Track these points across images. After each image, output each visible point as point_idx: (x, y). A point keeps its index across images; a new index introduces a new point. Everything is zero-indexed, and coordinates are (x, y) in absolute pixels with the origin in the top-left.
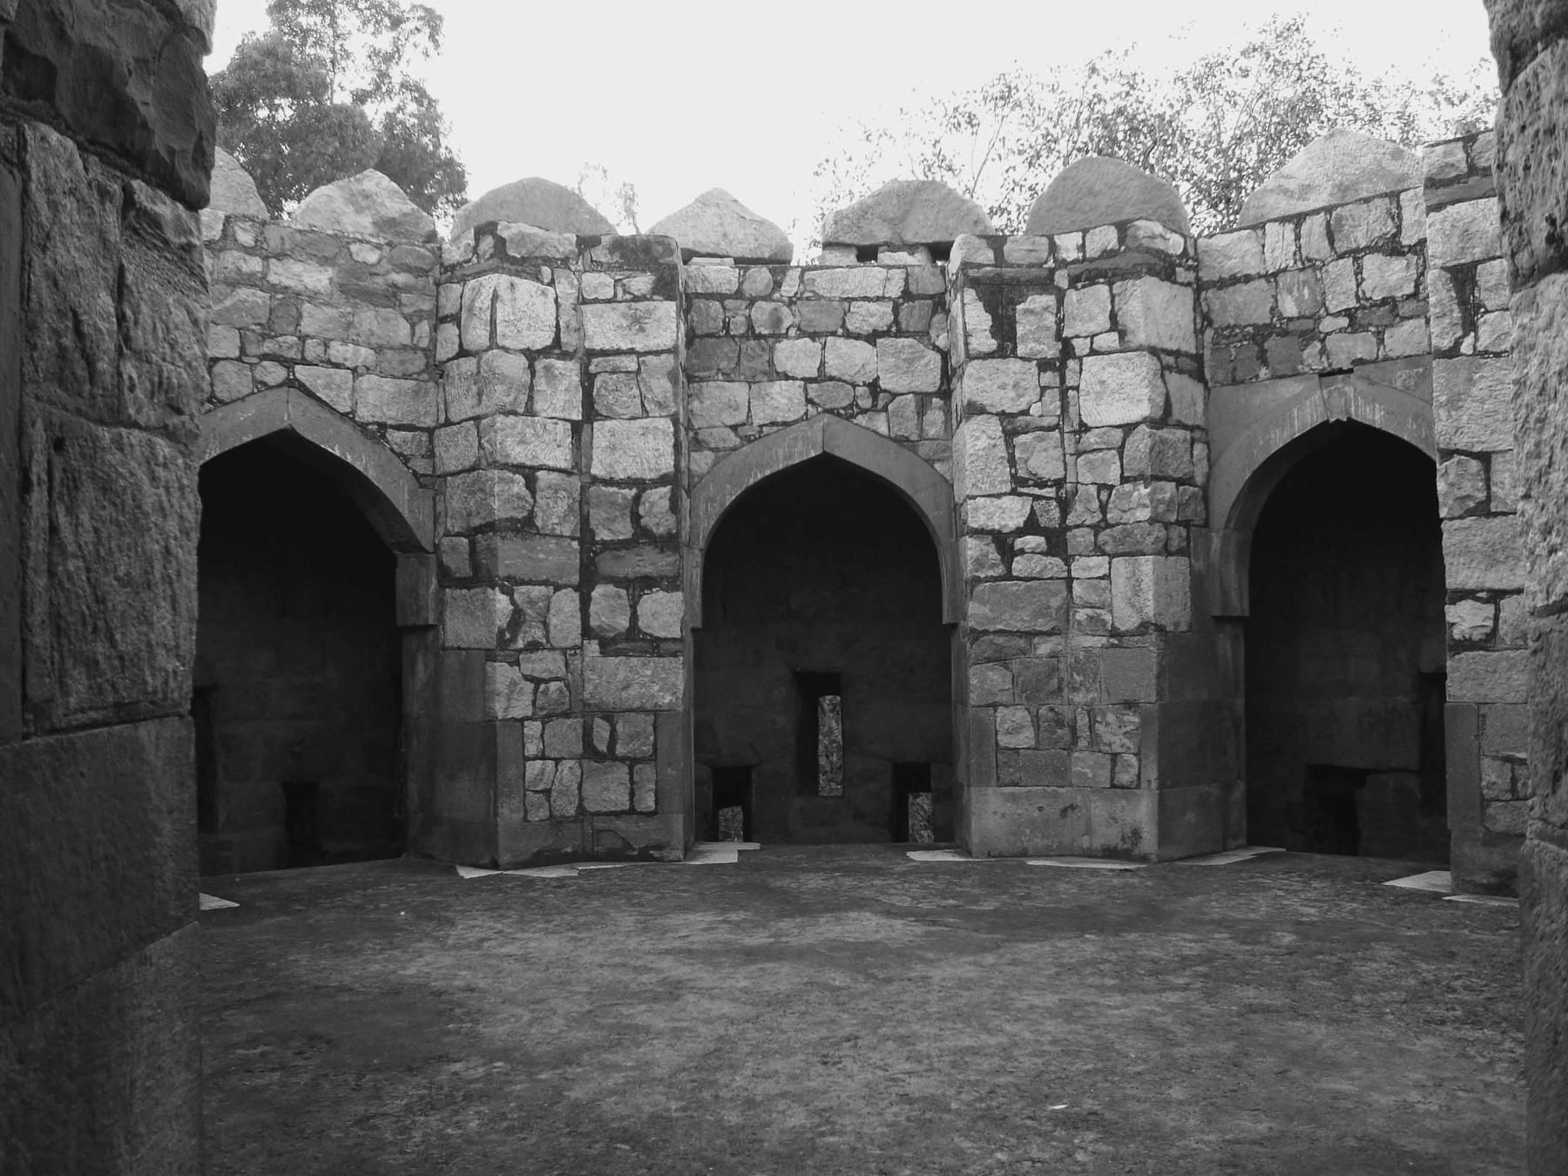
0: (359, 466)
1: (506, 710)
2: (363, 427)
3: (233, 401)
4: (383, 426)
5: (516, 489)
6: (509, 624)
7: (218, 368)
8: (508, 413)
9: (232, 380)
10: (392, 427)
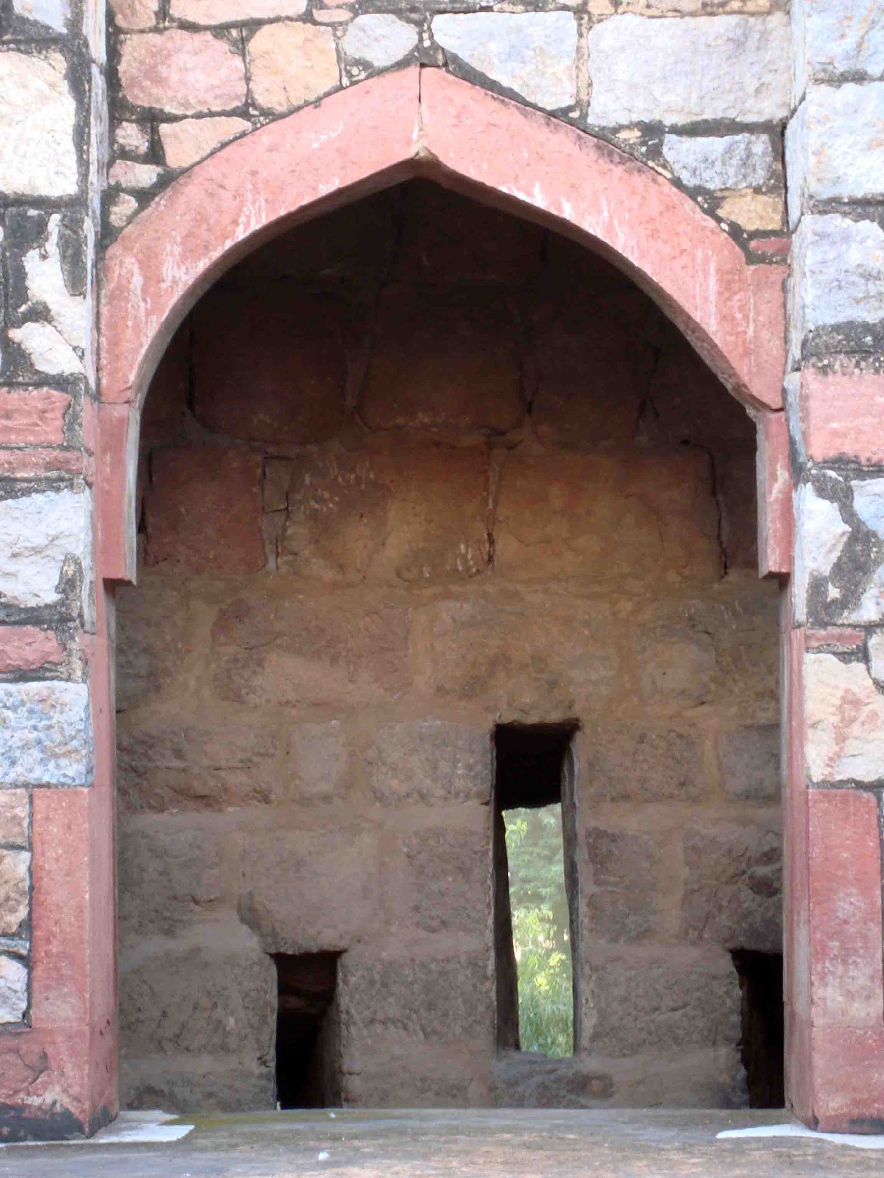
0: (593, 224)
1: (832, 761)
2: (605, 139)
3: (296, 110)
4: (652, 131)
5: (854, 256)
6: (838, 567)
7: (258, 43)
8: (837, 80)
9: (292, 63)
10: (677, 130)
